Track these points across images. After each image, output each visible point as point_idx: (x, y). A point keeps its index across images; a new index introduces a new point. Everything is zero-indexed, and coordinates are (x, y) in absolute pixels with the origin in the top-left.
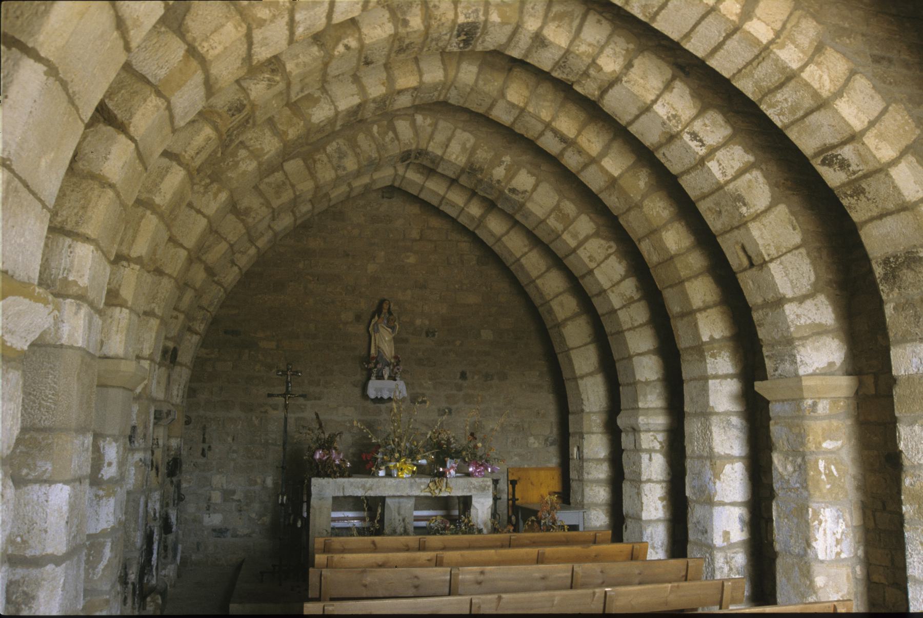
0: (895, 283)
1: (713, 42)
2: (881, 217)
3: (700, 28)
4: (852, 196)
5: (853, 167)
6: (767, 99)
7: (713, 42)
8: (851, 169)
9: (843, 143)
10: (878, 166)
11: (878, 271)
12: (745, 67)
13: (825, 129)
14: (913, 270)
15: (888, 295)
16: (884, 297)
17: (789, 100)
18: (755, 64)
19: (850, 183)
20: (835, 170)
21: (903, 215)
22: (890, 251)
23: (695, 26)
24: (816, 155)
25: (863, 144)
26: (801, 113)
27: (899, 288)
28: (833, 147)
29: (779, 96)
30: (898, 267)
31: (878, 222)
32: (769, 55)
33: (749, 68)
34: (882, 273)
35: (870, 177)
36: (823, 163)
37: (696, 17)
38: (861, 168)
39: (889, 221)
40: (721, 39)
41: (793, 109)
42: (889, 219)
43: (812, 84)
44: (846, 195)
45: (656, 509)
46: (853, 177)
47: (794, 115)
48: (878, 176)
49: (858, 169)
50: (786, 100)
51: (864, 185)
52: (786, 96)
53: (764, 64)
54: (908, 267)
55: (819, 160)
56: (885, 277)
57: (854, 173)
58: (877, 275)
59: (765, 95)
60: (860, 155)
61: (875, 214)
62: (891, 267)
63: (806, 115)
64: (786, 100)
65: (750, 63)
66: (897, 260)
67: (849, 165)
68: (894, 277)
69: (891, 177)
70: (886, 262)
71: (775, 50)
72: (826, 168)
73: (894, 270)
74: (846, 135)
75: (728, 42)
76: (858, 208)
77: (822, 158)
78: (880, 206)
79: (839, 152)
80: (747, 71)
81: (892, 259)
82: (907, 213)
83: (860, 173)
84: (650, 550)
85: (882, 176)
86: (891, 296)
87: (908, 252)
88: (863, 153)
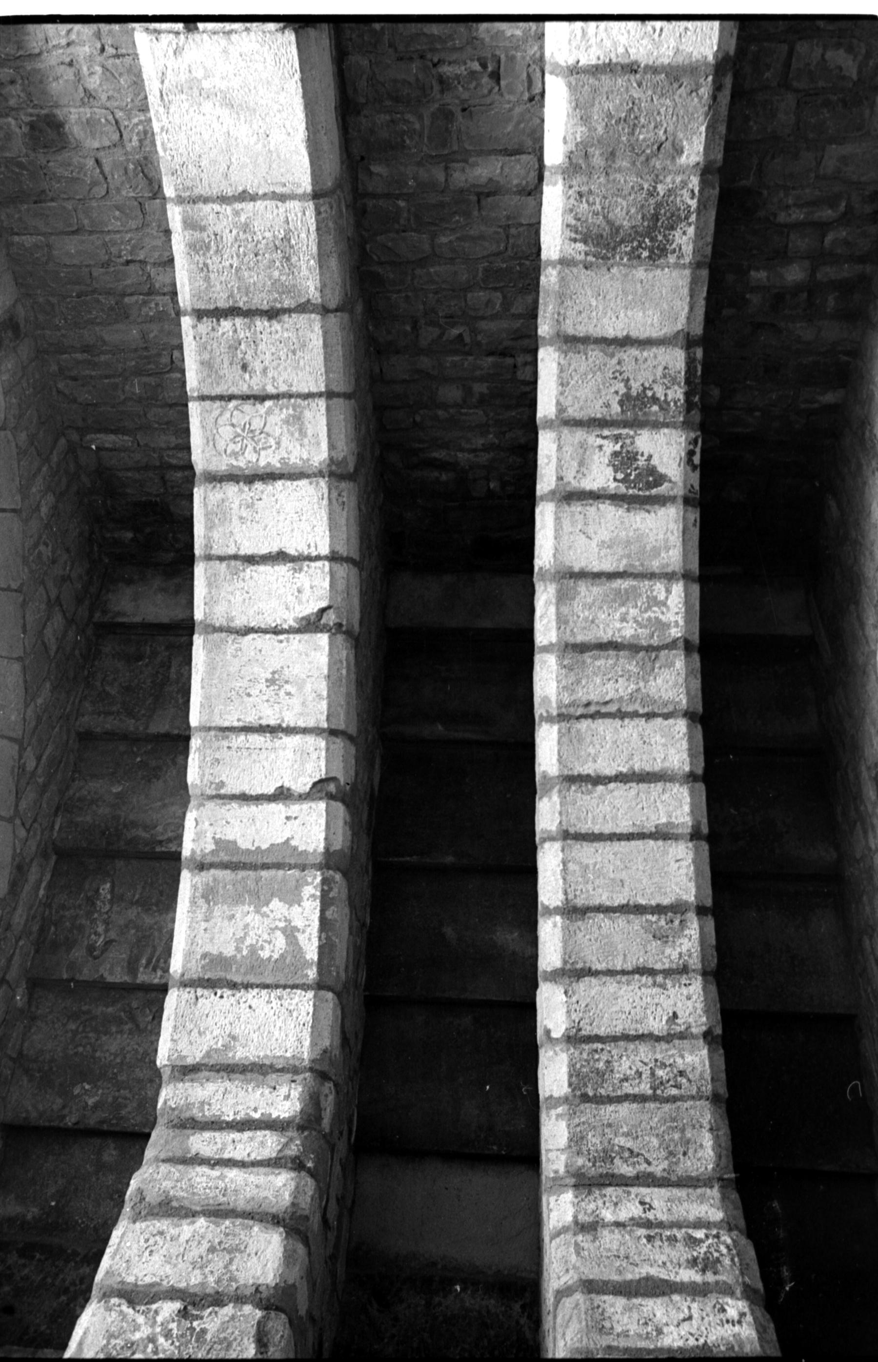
0: (659, 205)
1: (633, 792)
2: (626, 342)
3: (624, 826)
4: (655, 400)
5: (610, 447)
6: (655, 641)
7: (633, 792)
8: (618, 448)
9: (595, 496)
10: (566, 431)
11: (685, 239)
12: (635, 715)
13: (604, 535)
14: (610, 223)
15: (684, 184)
16: (695, 182)
17: (618, 616)
18: (613, 708)
19: (637, 424)
20: (650, 457)
21: (581, 331)
22: (640, 273)
23: (629, 837)
24: (662, 501)
25: (560, 478)
26: (618, 583)
27: (652, 193)
28: (615, 498)
29: (628, 631)
30: (636, 234)
31: (634, 334)
32: (572, 704)
33: (630, 709)
34: (677, 233)
35: (594, 420)
36: (660, 479)
37: (607, 849)
38: (599, 441)
39: (612, 328)
40: (612, 785)
41: (624, 598)
42: (610, 333)
43: (554, 617)
44: (664, 406)
45: (552, 821)
46: (624, 431)
47: (634, 588)
48: (578, 415)
49: (605, 442)
50: (623, 619)
51: (616, 408)
52: (618, 625)
53: (592, 697)
54: (616, 230)
55: (663, 489)
56: (675, 220)
57: (617, 438)
58: (691, 230)
59: (649, 649)
60: (581, 464)
61: (634, 352)
62: (652, 240)
63: (612, 576)
64: (623, 619)
65: (621, 715)
66: (634, 249)
67: (615, 454)
68: (656, 217)
69: (558, 403)
70: (659, 253)
71: (554, 705)
72: (662, 470)
73: (650, 232)
74: (577, 507)
75: (609, 771)
76: (659, 371)
77: (654, 491)
78: (614, 361)
79: (613, 485)
80: (637, 707)
81: (645, 254)
82: (570, 331)
83: (606, 432)
84: (555, 1197)
85: (573, 412)
86: (678, 179)
87: (605, 258)
88: (575, 464)
